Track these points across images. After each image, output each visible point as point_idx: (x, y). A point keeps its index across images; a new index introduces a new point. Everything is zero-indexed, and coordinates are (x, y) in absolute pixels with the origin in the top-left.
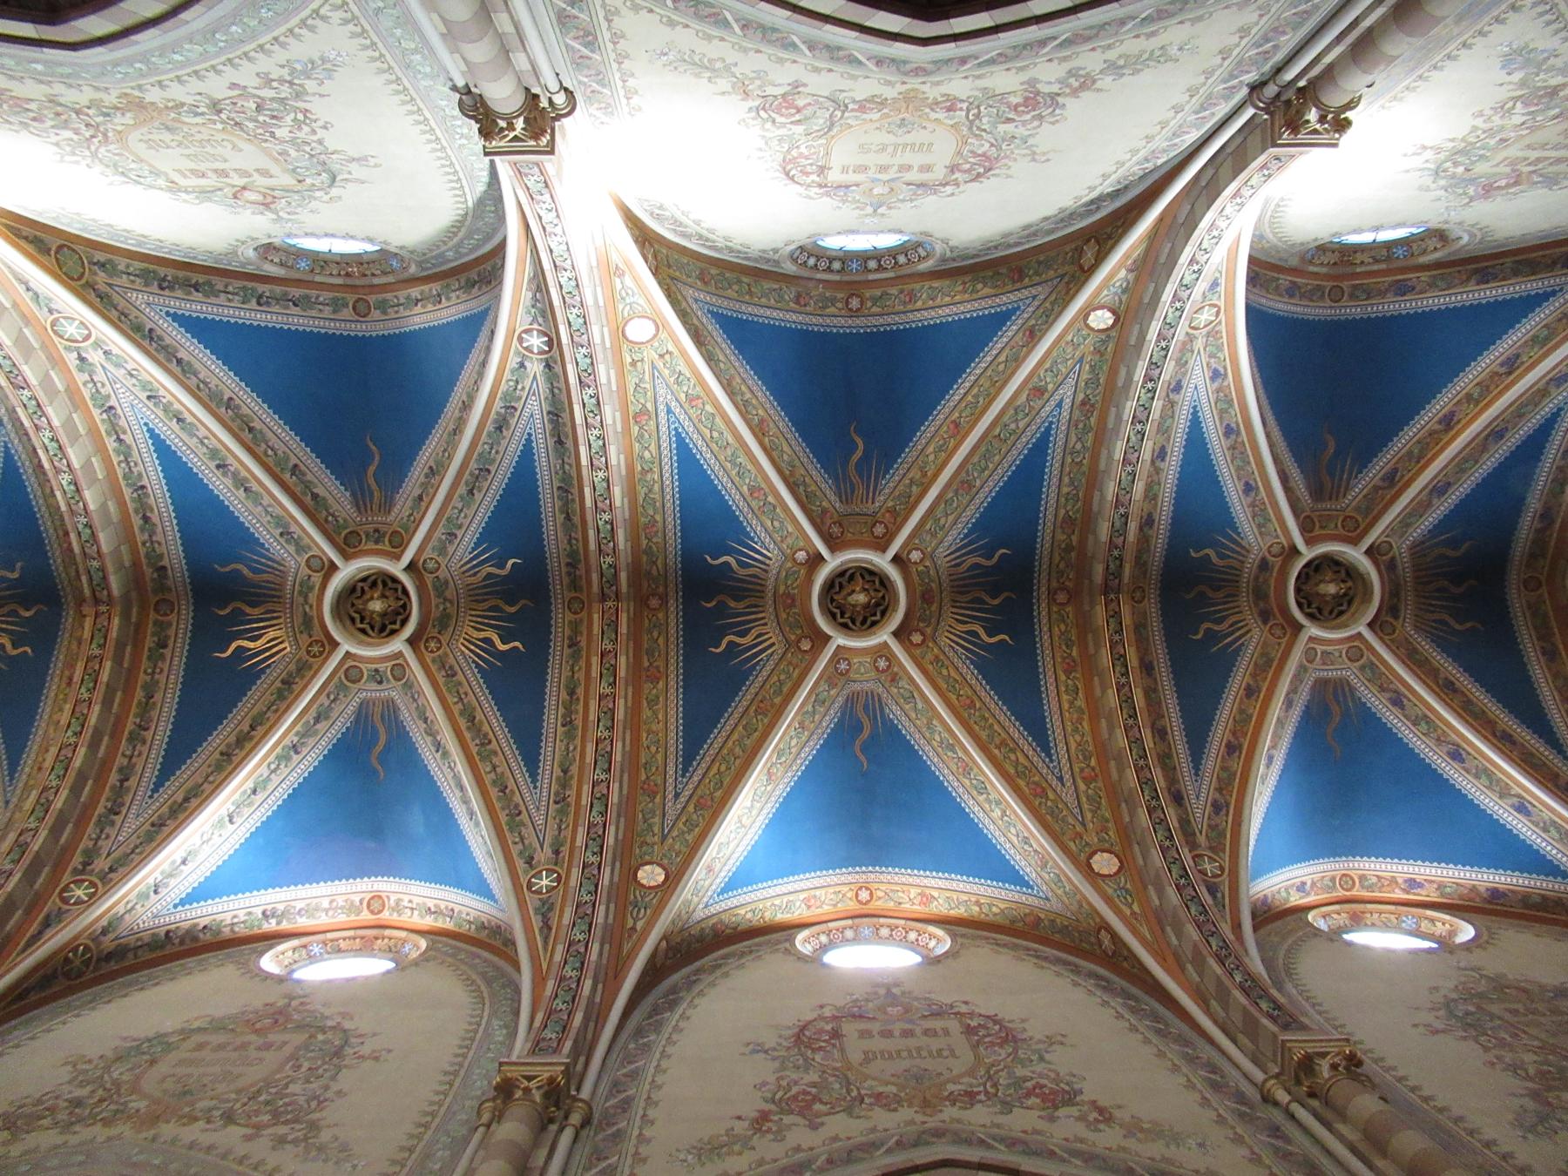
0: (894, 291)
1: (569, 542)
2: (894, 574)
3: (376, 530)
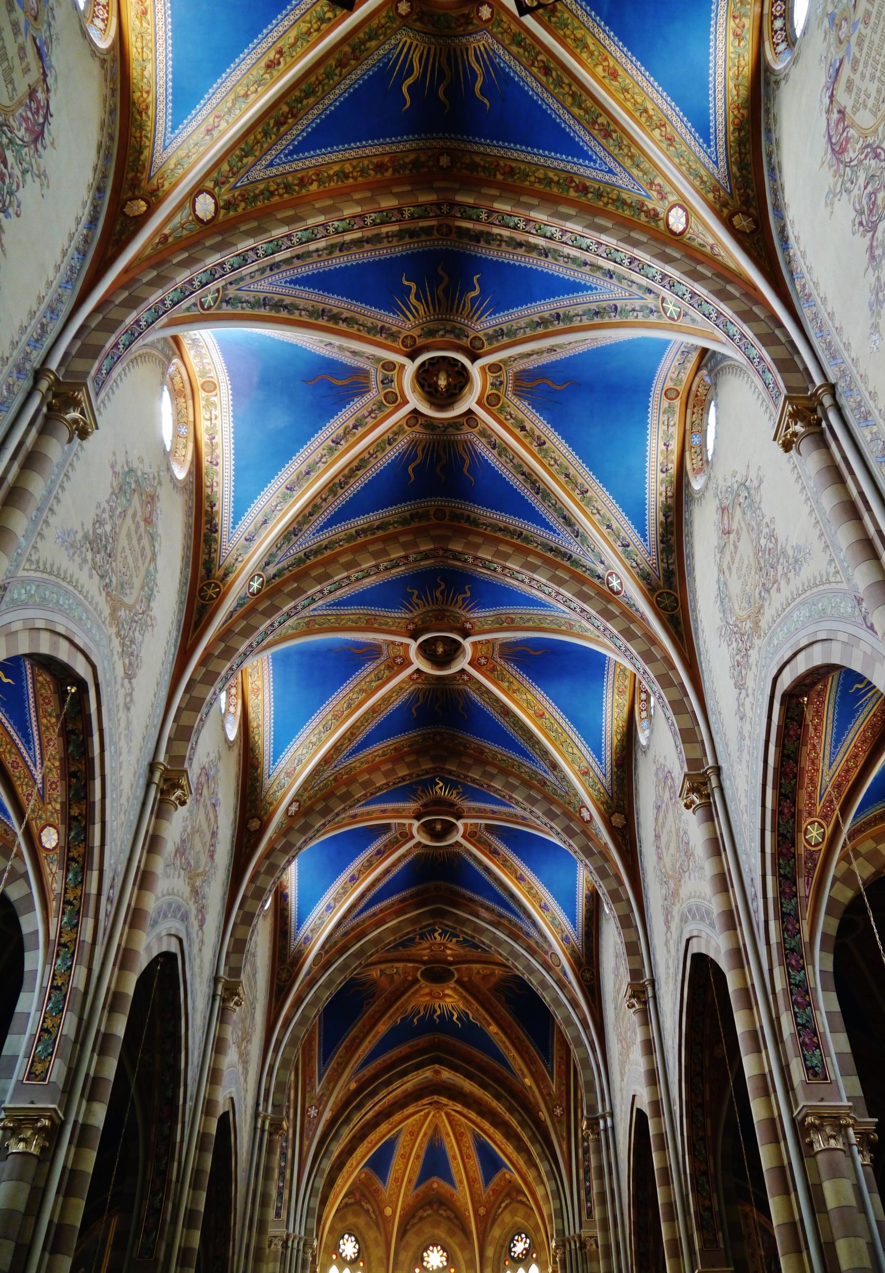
0: (627, 683)
1: (484, 524)
2: (459, 409)
3: (501, 383)
